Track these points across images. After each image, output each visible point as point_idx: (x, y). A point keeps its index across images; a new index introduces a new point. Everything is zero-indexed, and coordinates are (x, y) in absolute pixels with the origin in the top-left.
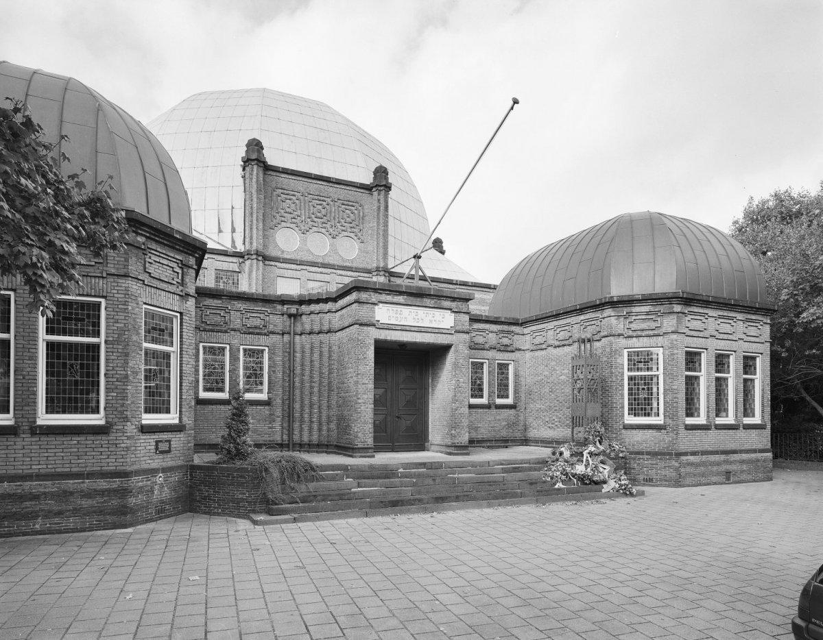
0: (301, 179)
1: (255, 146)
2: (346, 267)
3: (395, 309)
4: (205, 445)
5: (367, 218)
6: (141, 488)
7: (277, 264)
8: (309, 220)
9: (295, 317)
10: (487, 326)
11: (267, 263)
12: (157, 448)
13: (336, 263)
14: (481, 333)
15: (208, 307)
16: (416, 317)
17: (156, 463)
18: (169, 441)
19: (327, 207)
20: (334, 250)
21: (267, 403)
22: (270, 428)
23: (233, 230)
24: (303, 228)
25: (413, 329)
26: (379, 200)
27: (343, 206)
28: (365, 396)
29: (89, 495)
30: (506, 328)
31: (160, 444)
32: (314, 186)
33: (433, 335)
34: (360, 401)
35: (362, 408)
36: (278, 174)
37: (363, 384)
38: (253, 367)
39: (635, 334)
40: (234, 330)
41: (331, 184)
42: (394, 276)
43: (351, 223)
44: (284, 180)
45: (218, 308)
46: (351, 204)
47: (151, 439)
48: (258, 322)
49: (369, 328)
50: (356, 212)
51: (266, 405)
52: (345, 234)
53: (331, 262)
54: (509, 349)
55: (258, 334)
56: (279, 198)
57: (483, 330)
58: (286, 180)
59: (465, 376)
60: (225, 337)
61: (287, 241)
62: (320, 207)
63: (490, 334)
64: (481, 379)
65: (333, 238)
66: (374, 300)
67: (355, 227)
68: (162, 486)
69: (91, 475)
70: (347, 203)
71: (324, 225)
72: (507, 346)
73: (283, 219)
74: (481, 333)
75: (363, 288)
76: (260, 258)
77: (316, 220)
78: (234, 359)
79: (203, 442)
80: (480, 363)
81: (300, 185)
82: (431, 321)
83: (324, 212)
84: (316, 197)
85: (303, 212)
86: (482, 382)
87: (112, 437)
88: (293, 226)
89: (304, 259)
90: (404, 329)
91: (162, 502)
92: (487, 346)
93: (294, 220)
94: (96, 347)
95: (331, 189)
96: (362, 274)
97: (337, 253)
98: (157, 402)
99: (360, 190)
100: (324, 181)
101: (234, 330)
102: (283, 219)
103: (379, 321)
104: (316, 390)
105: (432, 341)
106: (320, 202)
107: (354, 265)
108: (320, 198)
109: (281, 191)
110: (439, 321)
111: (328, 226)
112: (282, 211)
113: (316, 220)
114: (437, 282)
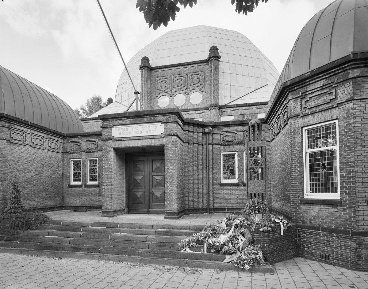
0: (169, 68)
1: (145, 60)
2: (195, 109)
3: (123, 128)
4: (72, 206)
5: (207, 78)
8: (174, 89)
10: (235, 128)
13: (189, 108)
14: (230, 134)
16: (149, 130)
19: (184, 79)
20: (188, 101)
24: (171, 94)
25: (135, 138)
26: (211, 66)
27: (193, 76)
28: (107, 182)
32: (176, 70)
33: (149, 140)
34: (104, 184)
35: (105, 188)
36: (158, 70)
37: (106, 174)
38: (93, 168)
41: (186, 66)
42: (225, 108)
43: (197, 84)
44: (160, 72)
46: (197, 73)
49: (109, 142)
50: (200, 77)
51: (97, 187)
52: (194, 91)
53: (186, 108)
57: (231, 131)
58: (162, 72)
59: (173, 165)
63: (239, 134)
64: (233, 165)
65: (187, 95)
66: (111, 125)
67: (200, 86)
70: (195, 73)
71: (182, 89)
73: (161, 92)
74: (230, 134)
75: (105, 119)
77: (177, 87)
79: (71, 205)
80: (231, 154)
81: (170, 71)
82: (147, 132)
83: (182, 82)
84: (177, 76)
85: (170, 86)
86: (234, 168)
90: (129, 139)
92: (235, 142)
95: (186, 69)
96: (204, 111)
97: (190, 102)
99: (203, 64)
100: (181, 66)
102: (161, 92)
103: (114, 137)
105: (148, 144)
106: (179, 78)
107: (200, 107)
108: (179, 75)
110: (153, 131)
111: (184, 89)
113: (177, 87)
114: (256, 105)
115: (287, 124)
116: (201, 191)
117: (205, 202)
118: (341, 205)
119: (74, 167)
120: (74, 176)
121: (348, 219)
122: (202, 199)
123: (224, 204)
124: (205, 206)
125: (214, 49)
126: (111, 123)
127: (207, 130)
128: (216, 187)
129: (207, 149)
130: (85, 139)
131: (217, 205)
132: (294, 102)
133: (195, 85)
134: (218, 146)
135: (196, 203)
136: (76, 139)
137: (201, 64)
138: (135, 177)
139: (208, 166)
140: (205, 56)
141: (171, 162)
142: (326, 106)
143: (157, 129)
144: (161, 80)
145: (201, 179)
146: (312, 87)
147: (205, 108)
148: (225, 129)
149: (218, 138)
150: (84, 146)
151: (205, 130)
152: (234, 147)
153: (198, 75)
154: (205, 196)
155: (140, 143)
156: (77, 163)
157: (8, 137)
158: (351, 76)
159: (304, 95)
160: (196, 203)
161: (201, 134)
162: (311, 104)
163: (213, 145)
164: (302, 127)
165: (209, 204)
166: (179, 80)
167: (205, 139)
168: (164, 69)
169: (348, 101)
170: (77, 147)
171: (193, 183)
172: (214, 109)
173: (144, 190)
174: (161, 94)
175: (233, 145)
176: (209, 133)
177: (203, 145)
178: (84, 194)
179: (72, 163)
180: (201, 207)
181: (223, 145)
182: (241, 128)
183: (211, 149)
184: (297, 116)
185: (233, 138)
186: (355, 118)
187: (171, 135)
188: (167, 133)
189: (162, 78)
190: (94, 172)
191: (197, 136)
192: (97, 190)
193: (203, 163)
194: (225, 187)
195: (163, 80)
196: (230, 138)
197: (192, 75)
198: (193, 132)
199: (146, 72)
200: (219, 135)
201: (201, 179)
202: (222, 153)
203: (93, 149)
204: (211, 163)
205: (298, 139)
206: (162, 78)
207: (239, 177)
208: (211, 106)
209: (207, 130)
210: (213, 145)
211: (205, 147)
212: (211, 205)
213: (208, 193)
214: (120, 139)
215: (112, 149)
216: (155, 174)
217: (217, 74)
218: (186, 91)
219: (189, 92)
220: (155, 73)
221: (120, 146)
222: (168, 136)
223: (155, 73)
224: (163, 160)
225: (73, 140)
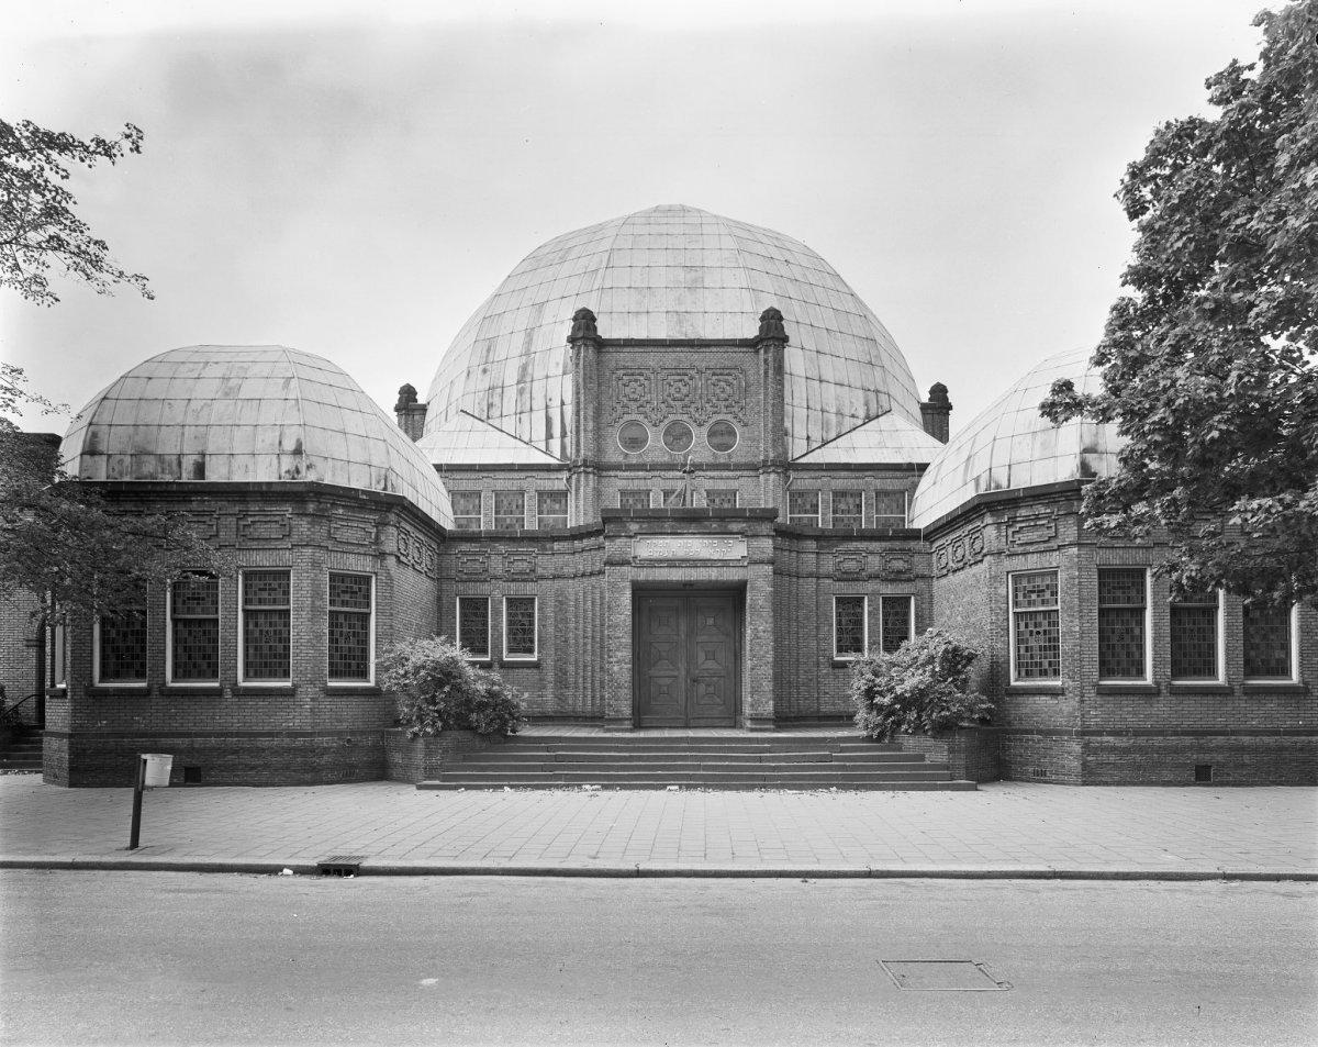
7: (619, 473)
11: (604, 473)
15: (465, 553)
21: (536, 665)
22: (539, 696)
23: (563, 435)
26: (766, 361)
27: (714, 378)
28: (619, 654)
30: (897, 544)
32: (671, 358)
39: (1020, 550)
44: (625, 357)
45: (475, 554)
54: (903, 577)
55: (523, 581)
56: (620, 382)
62: (680, 384)
72: (899, 572)
76: (590, 470)
78: (497, 613)
81: (652, 358)
83: (685, 390)
87: (298, 697)
94: (289, 611)
95: (696, 356)
102: (626, 409)
104: (589, 647)
106: (679, 377)
108: (680, 372)
112: (624, 399)
115: (981, 561)
121: (1071, 713)
130: (502, 548)
134: (827, 581)
137: (737, 349)
140: (751, 330)
141: (762, 616)
142: (1042, 547)
143: (737, 549)
144: (627, 378)
146: (1023, 512)
147: (746, 464)
148: (843, 547)
150: (497, 565)
153: (730, 378)
159: (1013, 521)
162: (1024, 537)
163: (818, 578)
164: (1008, 573)
168: (636, 349)
172: (773, 471)
175: (857, 580)
181: (839, 580)
182: (875, 546)
187: (762, 562)
188: (756, 557)
190: (524, 630)
196: (851, 565)
197: (714, 374)
198: (790, 551)
199: (589, 353)
205: (1002, 591)
208: (765, 464)
214: (653, 563)
217: (781, 383)
218: (697, 416)
222: (755, 563)
223: (614, 358)
225: (465, 547)
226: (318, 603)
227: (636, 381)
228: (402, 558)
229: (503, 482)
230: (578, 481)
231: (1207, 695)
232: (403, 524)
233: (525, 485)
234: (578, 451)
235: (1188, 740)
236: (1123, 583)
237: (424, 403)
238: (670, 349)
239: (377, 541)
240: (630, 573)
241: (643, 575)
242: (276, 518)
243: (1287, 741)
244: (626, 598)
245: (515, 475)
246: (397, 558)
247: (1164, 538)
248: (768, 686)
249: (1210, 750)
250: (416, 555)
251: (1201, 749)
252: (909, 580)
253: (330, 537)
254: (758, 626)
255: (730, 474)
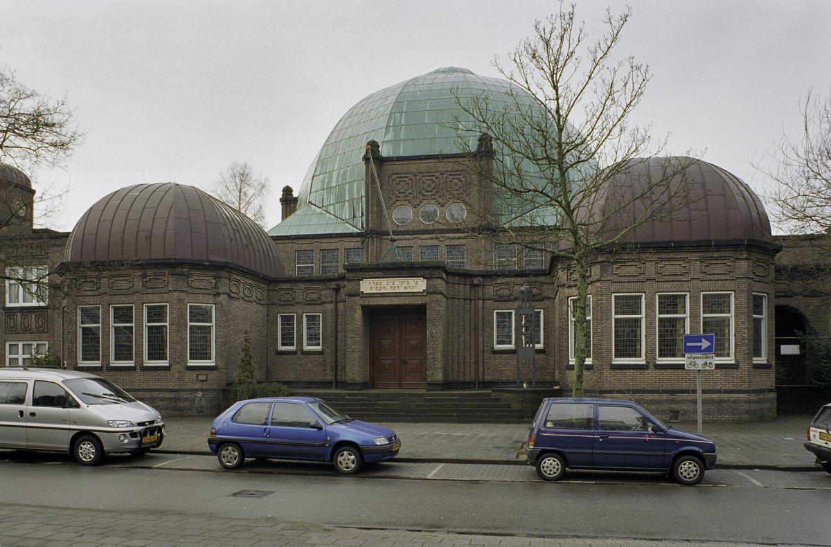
1: (373, 146)
6: (187, 398)
9: (337, 290)
12: (197, 378)
15: (282, 290)
17: (196, 387)
18: (206, 375)
22: (323, 370)
29: (162, 400)
31: (199, 377)
32: (424, 166)
40: (299, 303)
44: (397, 167)
47: (194, 373)
48: (314, 296)
57: (507, 284)
60: (292, 308)
61: (402, 215)
62: (430, 182)
65: (442, 206)
68: (201, 399)
69: (163, 390)
78: (300, 323)
81: (413, 167)
82: (406, 288)
83: (433, 185)
88: (406, 203)
89: (416, 229)
90: (383, 295)
91: (201, 407)
93: (406, 198)
98: (201, 351)
101: (299, 303)
106: (428, 178)
109: (397, 176)
111: (437, 197)
112: (397, 192)
116: (468, 359)
117: (473, 373)
118: (593, 369)
119: (282, 324)
120: (283, 339)
122: (469, 370)
123: (497, 377)
124: (473, 379)
125: (484, 140)
126: (360, 274)
127: (476, 281)
128: (487, 355)
129: (476, 306)
130: (302, 286)
131: (488, 378)
132: (562, 271)
133: (455, 193)
135: (461, 375)
136: (288, 286)
138: (382, 341)
139: (476, 328)
143: (418, 285)
145: (468, 344)
149: (490, 291)
150: (300, 296)
151: (473, 281)
152: (509, 304)
153: (460, 177)
154: (473, 366)
155: (396, 301)
156: (287, 320)
157: (228, 291)
158: (599, 260)
160: (461, 375)
161: (468, 286)
163: (484, 300)
165: (478, 377)
166: (428, 182)
167: (473, 292)
169: (598, 280)
170: (289, 297)
171: (458, 349)
173: (394, 357)
174: (398, 203)
176: (478, 285)
177: (471, 300)
178: (300, 364)
179: (279, 320)
180: (467, 380)
183: (481, 305)
184: (564, 285)
185: (510, 292)
186: (602, 295)
188: (430, 291)
189: (400, 176)
191: (463, 290)
192: (320, 358)
193: (470, 323)
194: (499, 355)
195: (401, 179)
196: (506, 292)
197: (450, 175)
200: (492, 287)
201: (468, 344)
202: (495, 311)
203: (313, 300)
204: (481, 323)
206: (400, 176)
207: (516, 342)
209: (476, 281)
210: (484, 300)
211: (473, 302)
212: (481, 377)
213: (476, 362)
214: (371, 295)
215: (359, 307)
216: (409, 337)
219: (444, 201)
220: (387, 167)
221: (371, 303)
222: (431, 293)
223: (389, 168)
224: (424, 320)
226: (182, 321)
227: (403, 181)
228: (233, 295)
229: (326, 245)
230: (368, 241)
231: (678, 369)
232: (235, 276)
233: (339, 245)
234: (367, 225)
235: (665, 396)
236: (629, 303)
237: (297, 196)
238: (424, 161)
239: (216, 287)
240: (359, 301)
241: (367, 302)
242: (160, 277)
243: (725, 396)
244: (358, 314)
245: (332, 240)
246: (229, 295)
247: (653, 276)
248: (439, 365)
249: (678, 402)
250: (247, 292)
251: (673, 401)
252: (540, 300)
253: (188, 286)
254: (435, 331)
255: (461, 235)
